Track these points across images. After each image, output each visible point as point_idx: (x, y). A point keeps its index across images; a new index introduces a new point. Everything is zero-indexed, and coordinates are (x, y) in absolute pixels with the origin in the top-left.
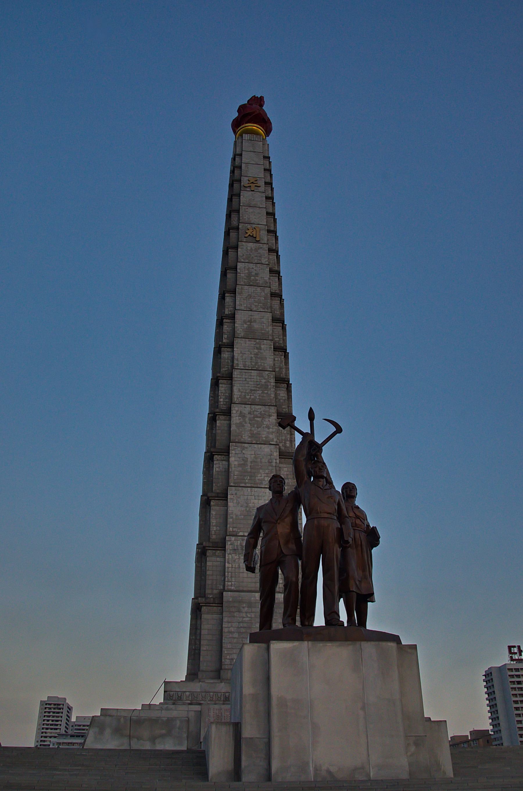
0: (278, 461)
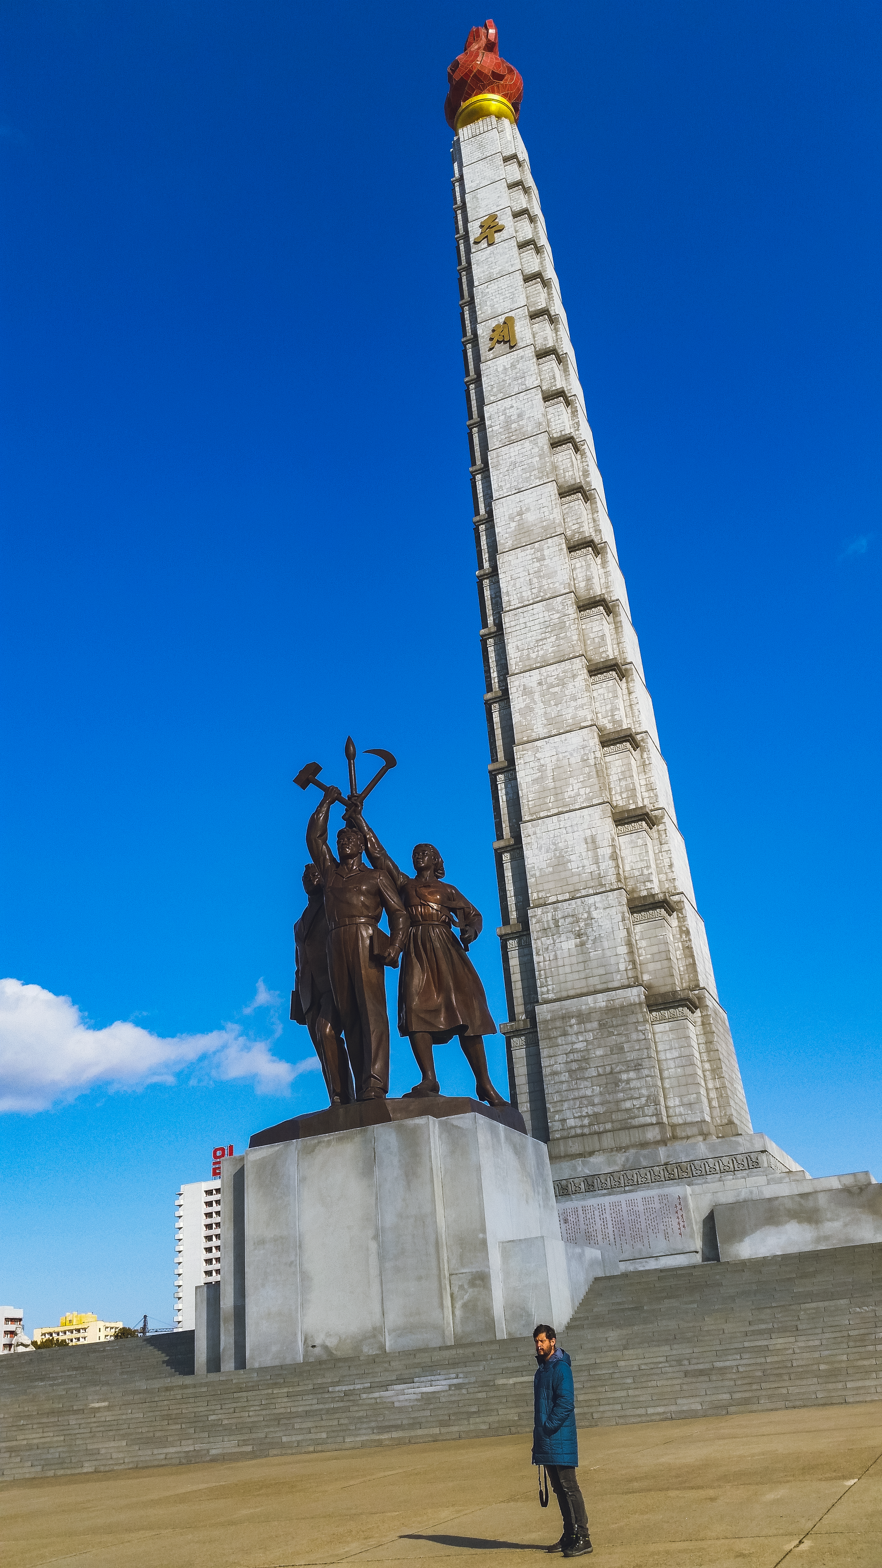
0: (598, 754)
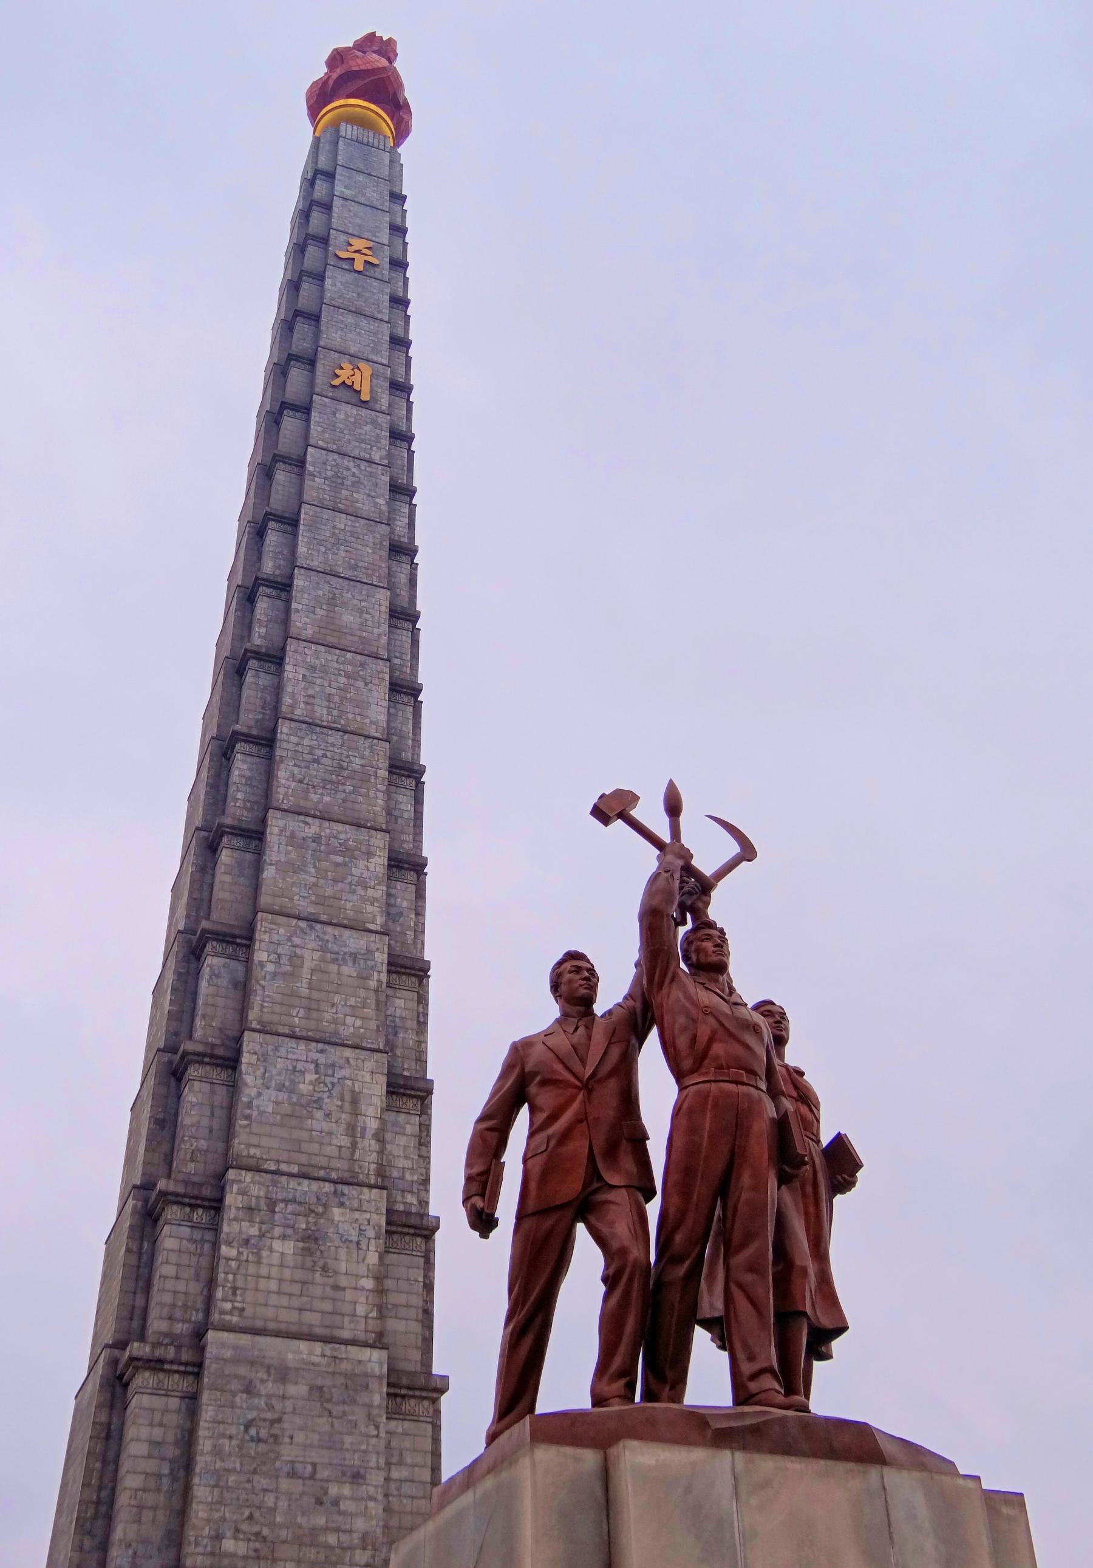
0: (384, 977)
